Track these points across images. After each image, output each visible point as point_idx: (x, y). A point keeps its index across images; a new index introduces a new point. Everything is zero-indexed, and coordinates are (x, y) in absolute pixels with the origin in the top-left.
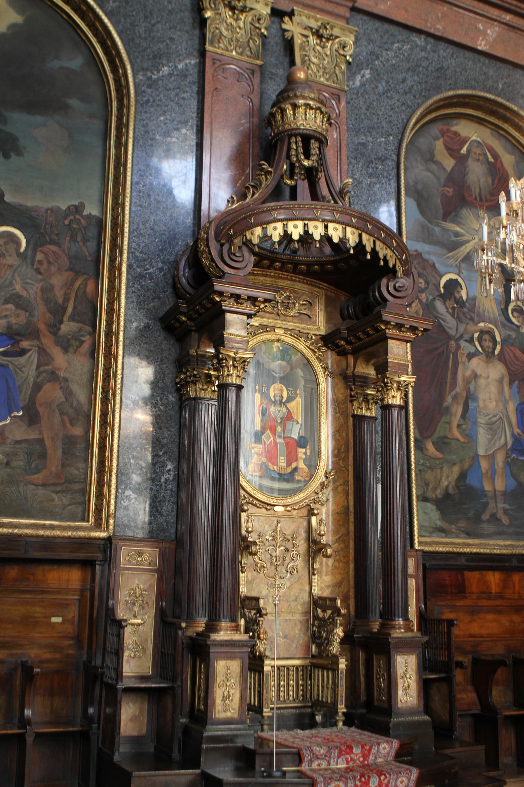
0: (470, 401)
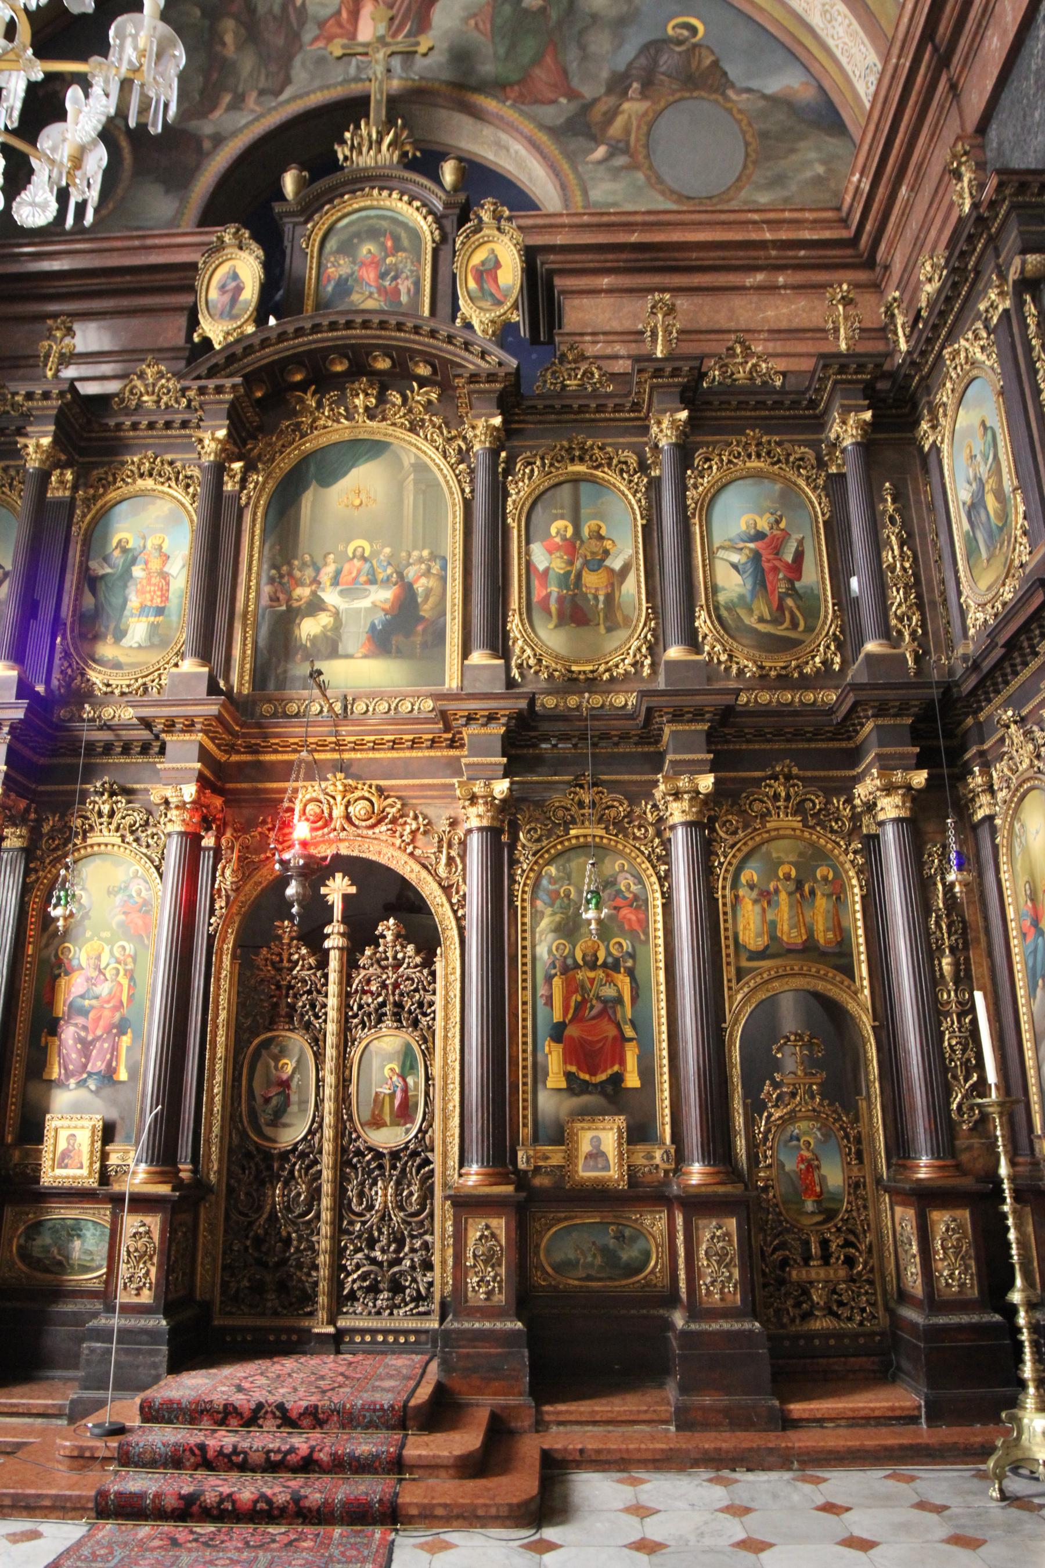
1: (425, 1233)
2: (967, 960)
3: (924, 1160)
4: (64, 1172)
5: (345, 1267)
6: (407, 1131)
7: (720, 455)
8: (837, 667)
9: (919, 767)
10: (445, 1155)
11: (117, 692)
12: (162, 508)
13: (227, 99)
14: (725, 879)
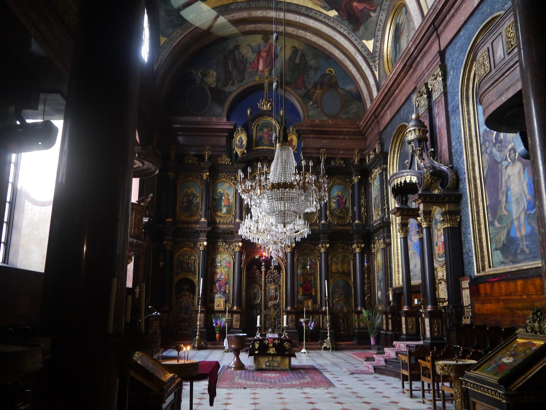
0: (508, 192)
2: (370, 275)
3: (359, 307)
4: (219, 308)
9: (363, 244)
11: (222, 222)
12: (227, 185)
13: (231, 82)
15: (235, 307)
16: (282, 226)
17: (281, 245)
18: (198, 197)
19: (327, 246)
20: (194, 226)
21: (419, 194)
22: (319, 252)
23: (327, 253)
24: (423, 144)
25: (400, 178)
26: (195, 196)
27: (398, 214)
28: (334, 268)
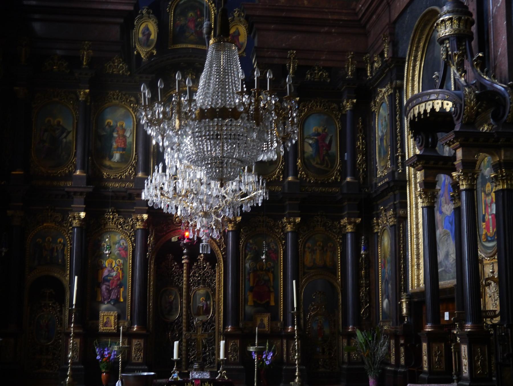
1: (213, 345)
3: (351, 327)
4: (107, 328)
5: (189, 355)
6: (208, 317)
7: (308, 105)
8: (339, 180)
9: (359, 217)
10: (219, 324)
11: (112, 177)
14: (301, 246)
15: (136, 326)
16: (219, 184)
17: (217, 218)
18: (69, 133)
19: (297, 220)
20: (62, 184)
21: (456, 132)
22: (283, 231)
23: (296, 233)
24: (465, 45)
25: (424, 104)
26: (63, 130)
27: (420, 166)
28: (308, 259)
